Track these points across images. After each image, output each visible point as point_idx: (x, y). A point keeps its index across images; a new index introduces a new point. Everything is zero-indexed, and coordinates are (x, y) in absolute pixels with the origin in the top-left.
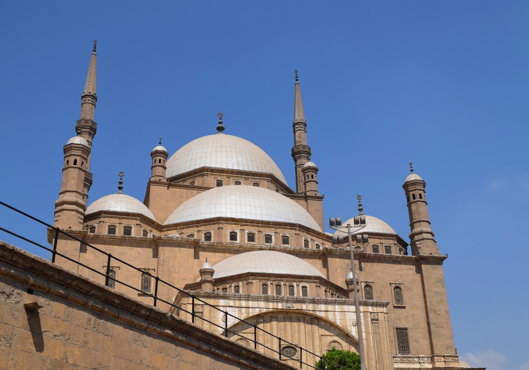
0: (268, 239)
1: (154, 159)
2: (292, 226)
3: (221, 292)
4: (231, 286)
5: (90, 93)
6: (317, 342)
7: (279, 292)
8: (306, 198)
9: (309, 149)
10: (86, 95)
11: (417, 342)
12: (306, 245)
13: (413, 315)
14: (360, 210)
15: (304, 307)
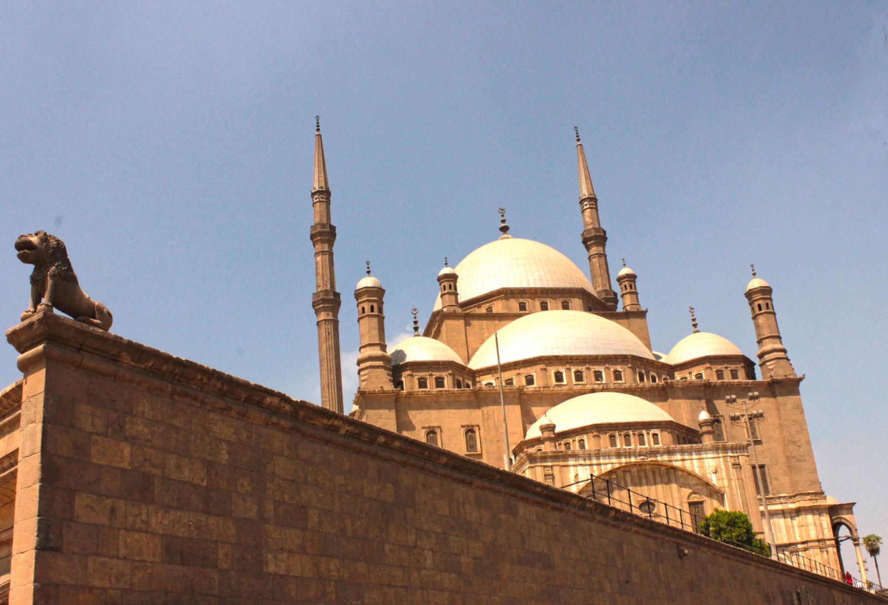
0: (598, 376)
1: (443, 285)
2: (623, 359)
3: (563, 448)
4: (574, 441)
5: (322, 187)
6: (676, 494)
7: (628, 443)
8: (627, 315)
9: (604, 232)
10: (318, 192)
11: (777, 479)
12: (642, 379)
13: (770, 449)
14: (695, 325)
15: (659, 459)
